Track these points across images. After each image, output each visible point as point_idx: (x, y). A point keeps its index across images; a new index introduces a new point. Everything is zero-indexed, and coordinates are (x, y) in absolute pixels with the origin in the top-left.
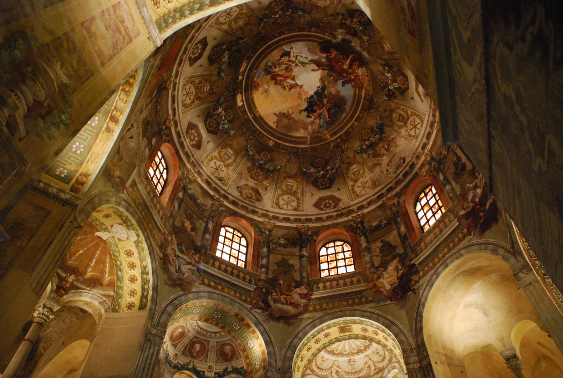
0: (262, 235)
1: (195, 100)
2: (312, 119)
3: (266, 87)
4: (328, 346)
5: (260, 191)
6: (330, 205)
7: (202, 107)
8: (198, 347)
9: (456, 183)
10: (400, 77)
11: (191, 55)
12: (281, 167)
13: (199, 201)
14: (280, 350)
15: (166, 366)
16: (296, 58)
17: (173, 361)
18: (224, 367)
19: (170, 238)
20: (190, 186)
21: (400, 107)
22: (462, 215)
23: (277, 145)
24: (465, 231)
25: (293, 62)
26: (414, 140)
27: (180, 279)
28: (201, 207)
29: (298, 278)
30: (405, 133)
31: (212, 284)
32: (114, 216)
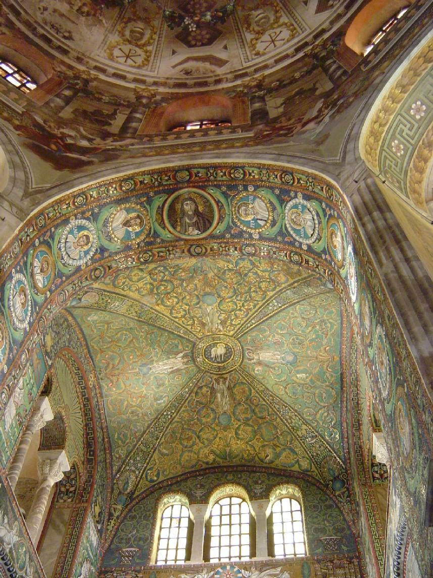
9: (73, 112)
10: (207, 34)
21: (155, 33)
22: (35, 119)
24: (17, 123)
26: (106, 55)
30: (113, 41)
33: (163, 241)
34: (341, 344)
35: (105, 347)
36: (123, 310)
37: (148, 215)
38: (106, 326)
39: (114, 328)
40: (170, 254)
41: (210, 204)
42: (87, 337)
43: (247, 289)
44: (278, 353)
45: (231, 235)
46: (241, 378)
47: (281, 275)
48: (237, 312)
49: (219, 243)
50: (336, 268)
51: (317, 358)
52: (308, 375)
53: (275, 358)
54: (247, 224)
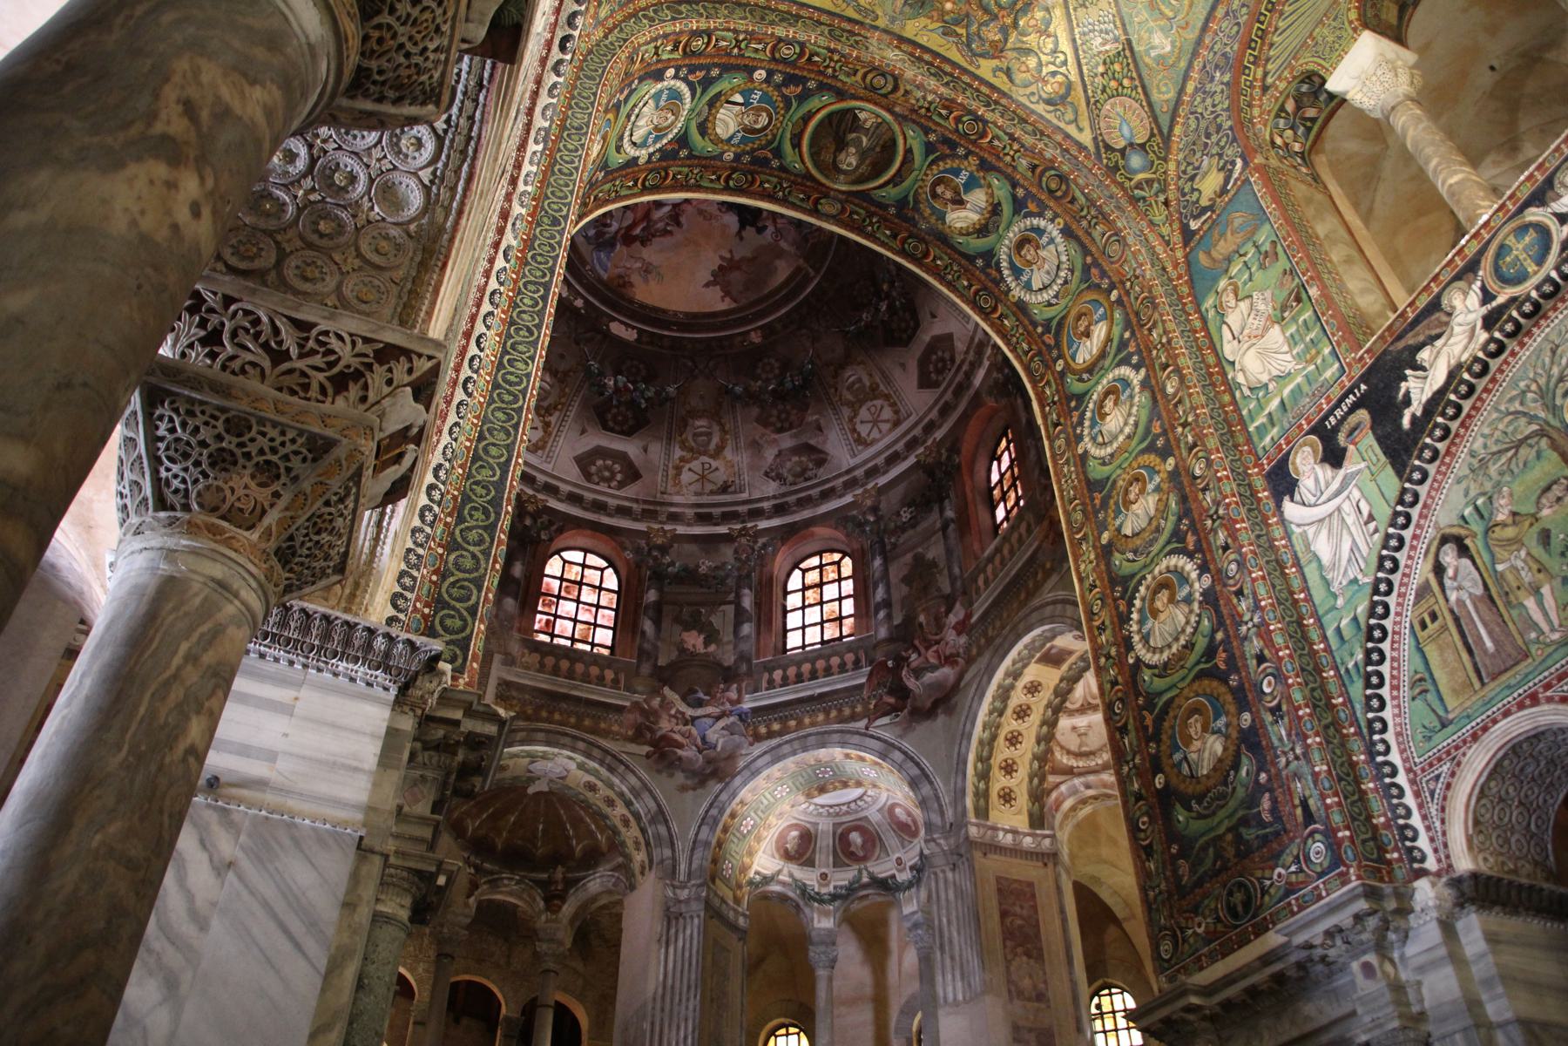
0: (864, 531)
2: (771, 229)
3: (638, 265)
4: (1064, 701)
5: (812, 442)
6: (942, 360)
7: (572, 414)
8: (856, 837)
12: (811, 362)
13: (703, 569)
14: (946, 783)
15: (812, 907)
17: (824, 891)
18: (917, 850)
19: (656, 702)
20: (668, 559)
23: (768, 330)
27: (709, 761)
29: (947, 589)
31: (776, 727)
33: (927, 131)
40: (931, 103)
41: (812, 145)
45: (804, 85)
49: (834, 77)
54: (765, 98)
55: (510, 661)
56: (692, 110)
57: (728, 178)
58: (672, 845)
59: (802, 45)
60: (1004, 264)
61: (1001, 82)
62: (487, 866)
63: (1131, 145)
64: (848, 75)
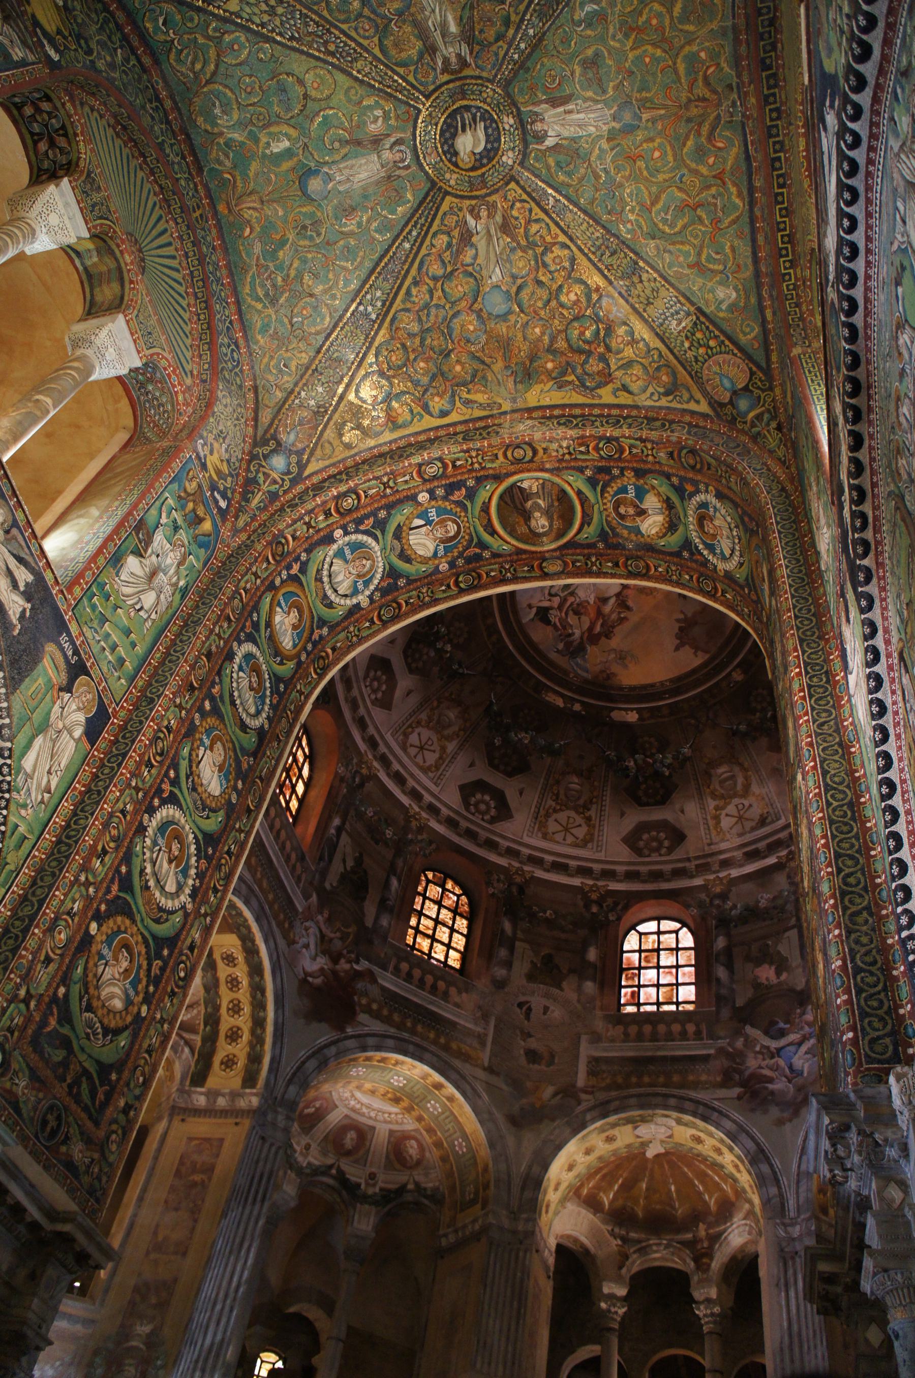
1: (587, 814)
3: (613, 656)
11: (487, 817)
16: (556, 595)
19: (740, 1043)
20: (730, 903)
25: (564, 600)
28: (775, 908)
32: (615, 1132)
33: (581, 470)
34: (226, 250)
35: (713, 190)
36: (668, 295)
37: (608, 516)
38: (704, 256)
39: (687, 248)
40: (568, 448)
41: (504, 527)
42: (747, 230)
43: (428, 341)
44: (341, 188)
46: (411, 78)
47: (369, 402)
48: (440, 272)
49: (483, 468)
50: (278, 582)
51: (262, 202)
52: (267, 151)
53: (346, 172)
55: (596, 1038)
56: (383, 549)
57: (457, 583)
58: (777, 1181)
59: (440, 459)
60: (701, 547)
61: (624, 399)
62: (633, 1235)
63: (735, 393)
64: (492, 461)
